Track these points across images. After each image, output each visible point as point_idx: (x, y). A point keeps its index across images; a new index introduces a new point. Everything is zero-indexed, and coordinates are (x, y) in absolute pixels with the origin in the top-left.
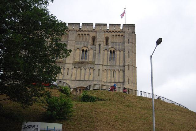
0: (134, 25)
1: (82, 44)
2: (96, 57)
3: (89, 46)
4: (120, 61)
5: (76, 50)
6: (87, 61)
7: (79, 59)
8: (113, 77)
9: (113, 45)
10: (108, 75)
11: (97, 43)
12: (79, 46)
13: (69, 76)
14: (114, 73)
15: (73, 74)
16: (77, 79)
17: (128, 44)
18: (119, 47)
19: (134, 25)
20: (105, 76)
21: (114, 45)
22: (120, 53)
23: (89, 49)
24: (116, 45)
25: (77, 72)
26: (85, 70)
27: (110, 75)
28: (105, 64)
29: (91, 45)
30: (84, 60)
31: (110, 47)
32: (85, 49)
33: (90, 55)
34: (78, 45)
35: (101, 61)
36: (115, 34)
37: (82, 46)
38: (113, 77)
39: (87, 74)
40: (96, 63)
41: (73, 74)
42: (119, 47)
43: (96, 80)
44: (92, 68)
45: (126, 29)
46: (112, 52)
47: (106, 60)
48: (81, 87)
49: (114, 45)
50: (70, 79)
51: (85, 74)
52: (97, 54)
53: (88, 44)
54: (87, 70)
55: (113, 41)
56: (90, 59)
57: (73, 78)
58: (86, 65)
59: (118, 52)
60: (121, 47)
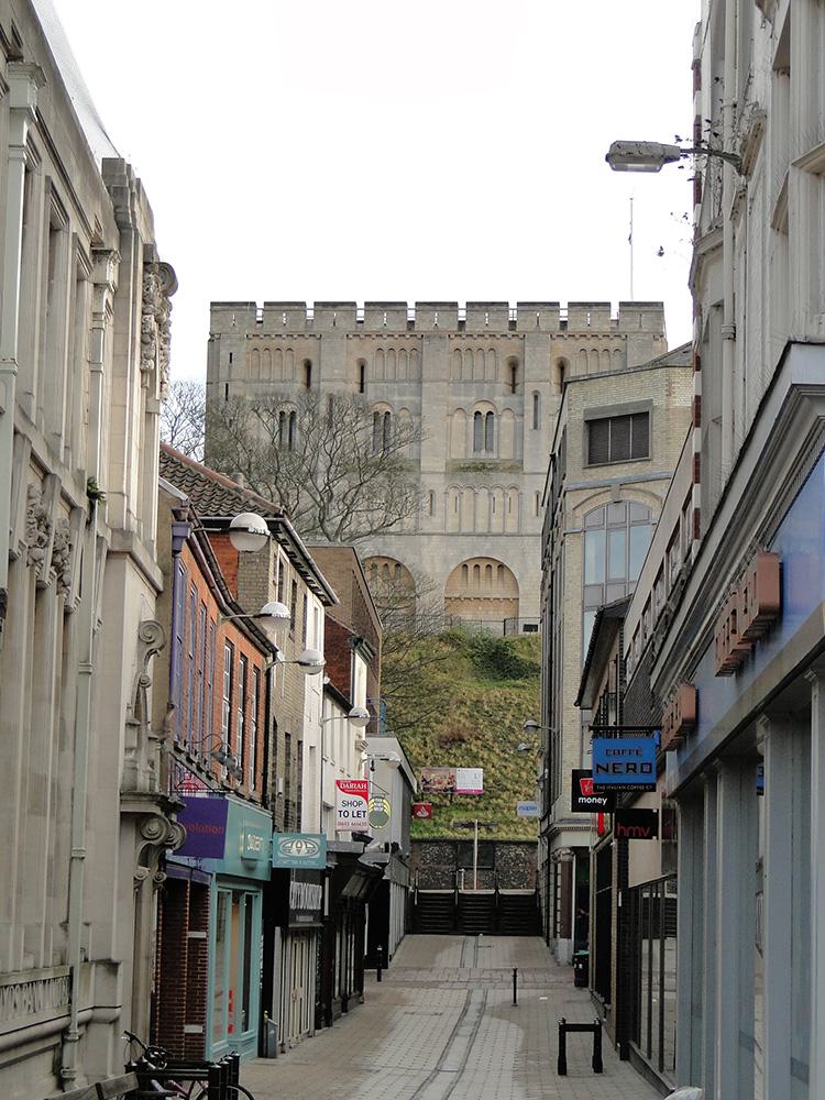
0: (662, 303)
2: (526, 446)
3: (500, 400)
5: (452, 415)
7: (466, 450)
11: (529, 388)
12: (462, 398)
13: (437, 520)
19: (662, 303)
23: (500, 409)
25: (464, 502)
29: (504, 395)
30: (483, 454)
32: (484, 410)
33: (502, 432)
34: (460, 395)
40: (527, 467)
41: (451, 510)
43: (530, 532)
45: (631, 325)
52: (527, 433)
54: (497, 493)
56: (504, 451)
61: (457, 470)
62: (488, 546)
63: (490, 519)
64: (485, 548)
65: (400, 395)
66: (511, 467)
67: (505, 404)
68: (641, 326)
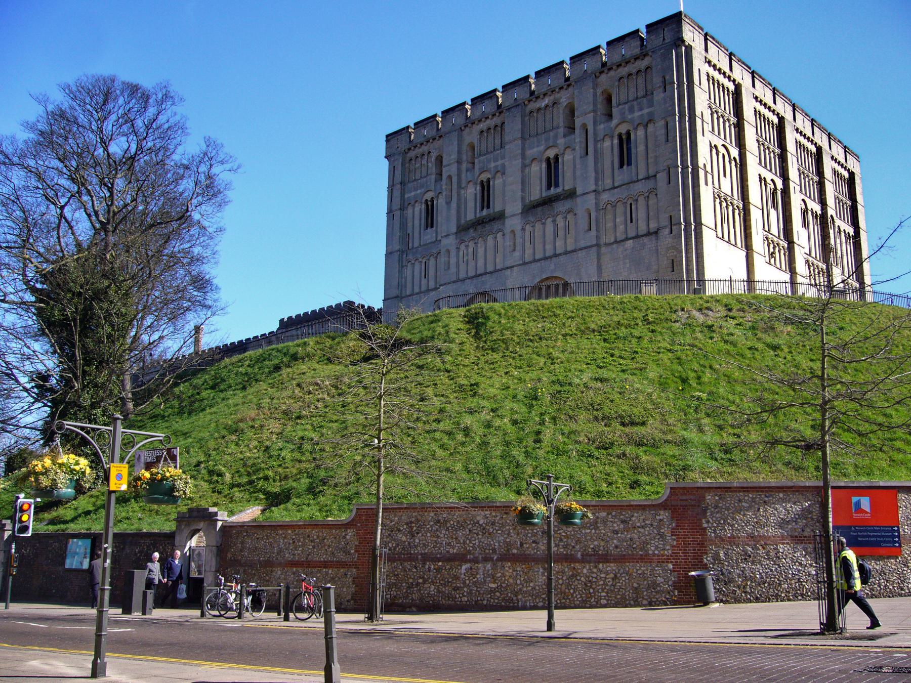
1: (543, 142)
2: (578, 173)
4: (647, 158)
6: (559, 190)
8: (631, 222)
9: (624, 113)
10: (618, 220)
11: (578, 122)
12: (535, 150)
13: (517, 254)
14: (633, 207)
15: (527, 244)
16: (537, 258)
17: (662, 95)
18: (640, 113)
20: (610, 225)
21: (627, 112)
22: (646, 133)
24: (631, 110)
26: (554, 221)
27: (623, 219)
28: (608, 182)
30: (553, 191)
31: (615, 122)
32: (551, 153)
35: (592, 181)
36: (624, 71)
37: (542, 148)
38: (631, 222)
39: (561, 233)
40: (579, 191)
41: (527, 244)
42: (640, 113)
43: (583, 246)
44: (570, 211)
46: (625, 142)
47: (608, 173)
48: (547, 279)
49: (627, 112)
50: (521, 262)
51: (556, 234)
53: (556, 137)
55: (623, 98)
57: (526, 256)
58: (555, 205)
59: (641, 133)
60: (646, 111)
61: (529, 209)
62: (552, 267)
63: (555, 244)
64: (550, 269)
65: (494, 162)
66: (570, 194)
67: (565, 144)
68: (664, 39)
